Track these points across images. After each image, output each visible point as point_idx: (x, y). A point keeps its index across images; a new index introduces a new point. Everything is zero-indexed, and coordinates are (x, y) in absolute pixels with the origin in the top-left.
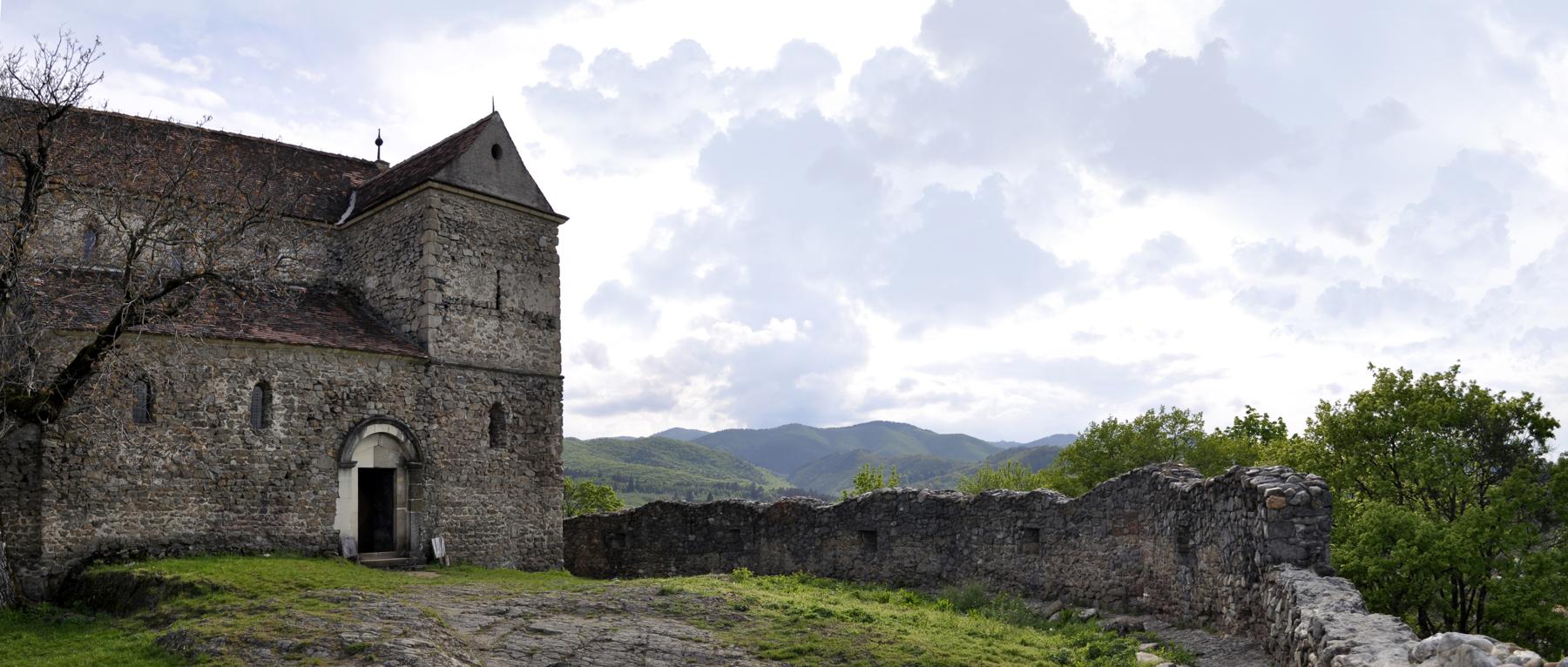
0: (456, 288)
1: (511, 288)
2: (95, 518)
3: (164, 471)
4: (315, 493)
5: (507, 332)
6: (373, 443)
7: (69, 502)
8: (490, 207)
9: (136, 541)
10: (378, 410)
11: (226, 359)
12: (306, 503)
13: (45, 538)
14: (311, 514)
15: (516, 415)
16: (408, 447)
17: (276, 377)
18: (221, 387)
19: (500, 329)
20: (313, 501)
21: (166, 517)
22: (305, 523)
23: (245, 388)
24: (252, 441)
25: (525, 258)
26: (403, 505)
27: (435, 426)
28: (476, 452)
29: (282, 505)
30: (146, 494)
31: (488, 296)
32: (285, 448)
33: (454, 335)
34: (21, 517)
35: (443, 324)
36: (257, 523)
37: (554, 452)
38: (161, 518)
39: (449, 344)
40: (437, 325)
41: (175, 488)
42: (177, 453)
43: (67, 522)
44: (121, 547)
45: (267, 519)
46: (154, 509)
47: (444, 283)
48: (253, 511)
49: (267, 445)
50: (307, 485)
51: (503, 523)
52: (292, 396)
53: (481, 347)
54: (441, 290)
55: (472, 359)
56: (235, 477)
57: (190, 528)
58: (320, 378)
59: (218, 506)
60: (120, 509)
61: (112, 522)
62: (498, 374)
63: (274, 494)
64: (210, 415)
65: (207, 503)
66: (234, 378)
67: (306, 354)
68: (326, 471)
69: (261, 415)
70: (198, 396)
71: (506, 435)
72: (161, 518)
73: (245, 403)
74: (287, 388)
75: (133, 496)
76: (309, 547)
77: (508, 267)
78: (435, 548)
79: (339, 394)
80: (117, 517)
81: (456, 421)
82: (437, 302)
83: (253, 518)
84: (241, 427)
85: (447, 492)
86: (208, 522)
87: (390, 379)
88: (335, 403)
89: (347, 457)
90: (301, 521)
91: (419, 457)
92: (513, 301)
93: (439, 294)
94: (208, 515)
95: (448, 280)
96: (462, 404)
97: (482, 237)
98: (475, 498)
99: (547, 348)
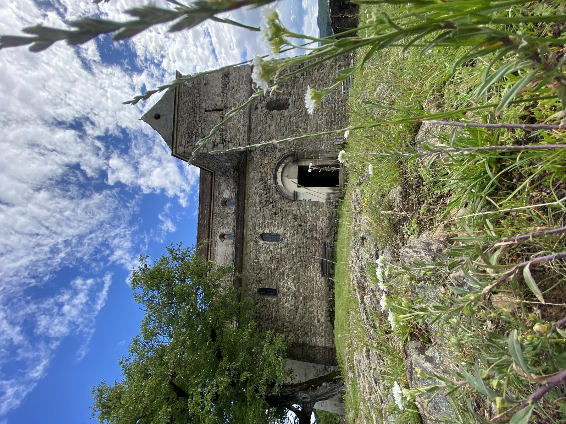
1: (213, 103)
2: (316, 321)
4: (308, 212)
6: (287, 180)
8: (179, 119)
12: (313, 216)
16: (288, 161)
18: (263, 258)
21: (317, 286)
24: (285, 243)
28: (290, 118)
29: (313, 229)
30: (306, 296)
33: (236, 136)
46: (313, 293)
47: (214, 143)
48: (315, 244)
50: (304, 217)
51: (328, 96)
54: (217, 144)
56: (300, 252)
58: (258, 209)
62: (252, 107)
63: (308, 233)
67: (248, 216)
68: (298, 206)
69: (275, 238)
70: (266, 268)
71: (282, 99)
73: (269, 247)
74: (261, 225)
75: (307, 302)
77: (203, 105)
88: (268, 201)
89: (292, 195)
91: (293, 155)
92: (218, 101)
93: (219, 145)
96: (267, 129)
97: (192, 122)
99: (238, 76)
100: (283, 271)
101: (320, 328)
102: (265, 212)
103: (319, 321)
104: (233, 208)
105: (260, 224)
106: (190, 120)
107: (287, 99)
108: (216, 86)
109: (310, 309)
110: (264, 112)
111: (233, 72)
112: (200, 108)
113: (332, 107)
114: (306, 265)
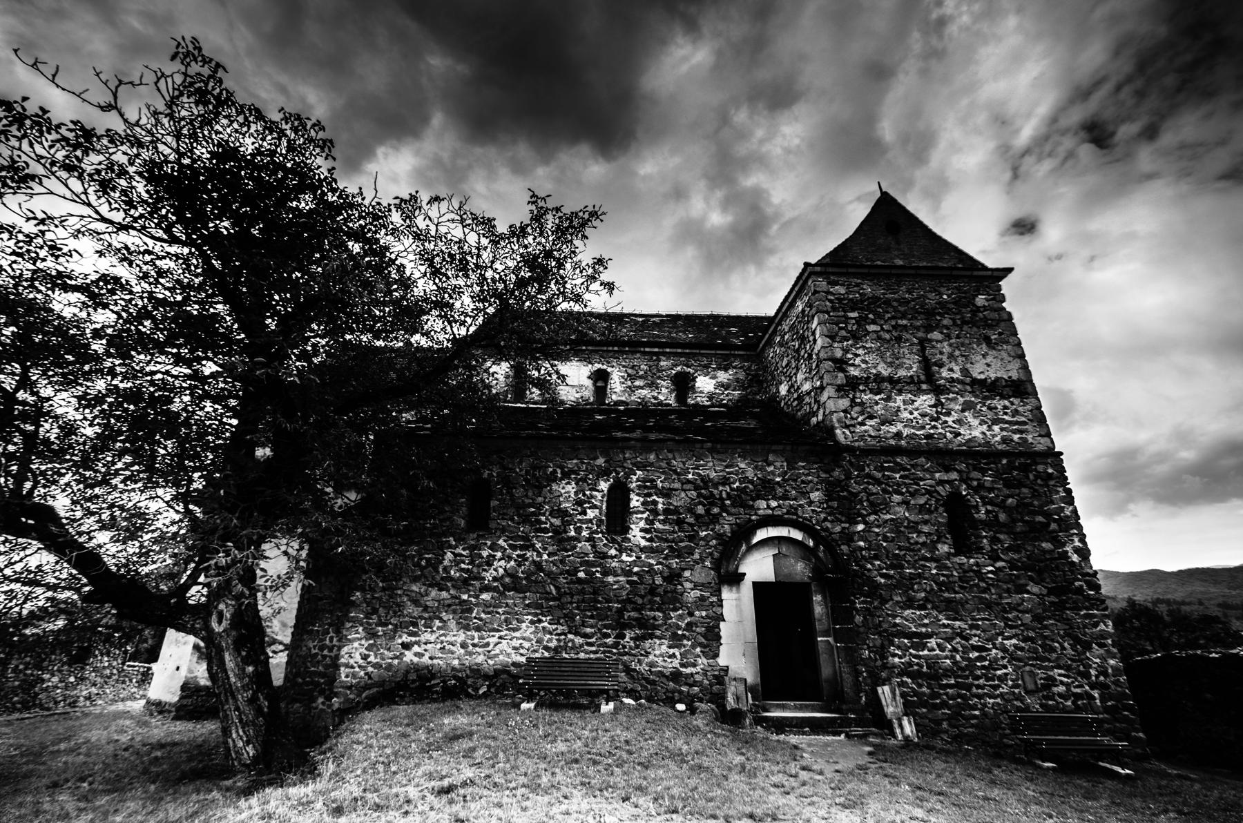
0: (863, 366)
2: (406, 638)
3: (495, 584)
4: (691, 614)
5: (951, 406)
7: (379, 617)
9: (453, 669)
10: (773, 509)
11: (575, 461)
12: (679, 628)
13: (342, 660)
14: (685, 642)
15: (989, 508)
16: (821, 555)
17: (634, 478)
19: (938, 404)
20: (687, 624)
21: (495, 640)
22: (677, 654)
23: (598, 491)
24: (605, 550)
25: (959, 322)
26: (826, 634)
27: (860, 527)
30: (470, 610)
31: (911, 367)
32: (647, 557)
33: (871, 417)
34: (331, 634)
35: (851, 406)
36: (609, 652)
37: (1075, 558)
38: (487, 640)
39: (863, 428)
40: (843, 408)
41: (507, 605)
42: (512, 563)
43: (372, 642)
44: (433, 676)
45: (624, 647)
46: (478, 629)
47: (846, 363)
48: (607, 636)
49: (624, 554)
51: (1005, 667)
52: (655, 497)
53: (913, 427)
55: (903, 443)
56: (582, 592)
57: (522, 655)
58: (690, 476)
59: (560, 627)
60: (439, 628)
61: (426, 644)
64: (553, 520)
65: (545, 624)
66: (584, 480)
67: (670, 451)
68: (703, 585)
69: (617, 519)
72: (487, 640)
73: (595, 507)
74: (647, 487)
75: (454, 612)
76: (684, 689)
77: (936, 335)
78: (884, 703)
79: (715, 492)
80: (432, 638)
81: (892, 520)
82: (839, 382)
83: (605, 645)
84: (592, 533)
85: (895, 617)
86: (547, 648)
87: (786, 473)
90: (671, 651)
92: (951, 370)
93: (841, 375)
94: (546, 639)
95: (850, 359)
98: (945, 626)
99: (1023, 419)
100: (533, 545)
101: (389, 649)
102: (683, 495)
103: (406, 646)
104: (672, 401)
105: (652, 481)
106: (895, 304)
107: (980, 550)
108: (988, 365)
109: (437, 623)
110: (940, 488)
111: (1029, 407)
112: (929, 329)
113: (978, 678)
114: (550, 611)
